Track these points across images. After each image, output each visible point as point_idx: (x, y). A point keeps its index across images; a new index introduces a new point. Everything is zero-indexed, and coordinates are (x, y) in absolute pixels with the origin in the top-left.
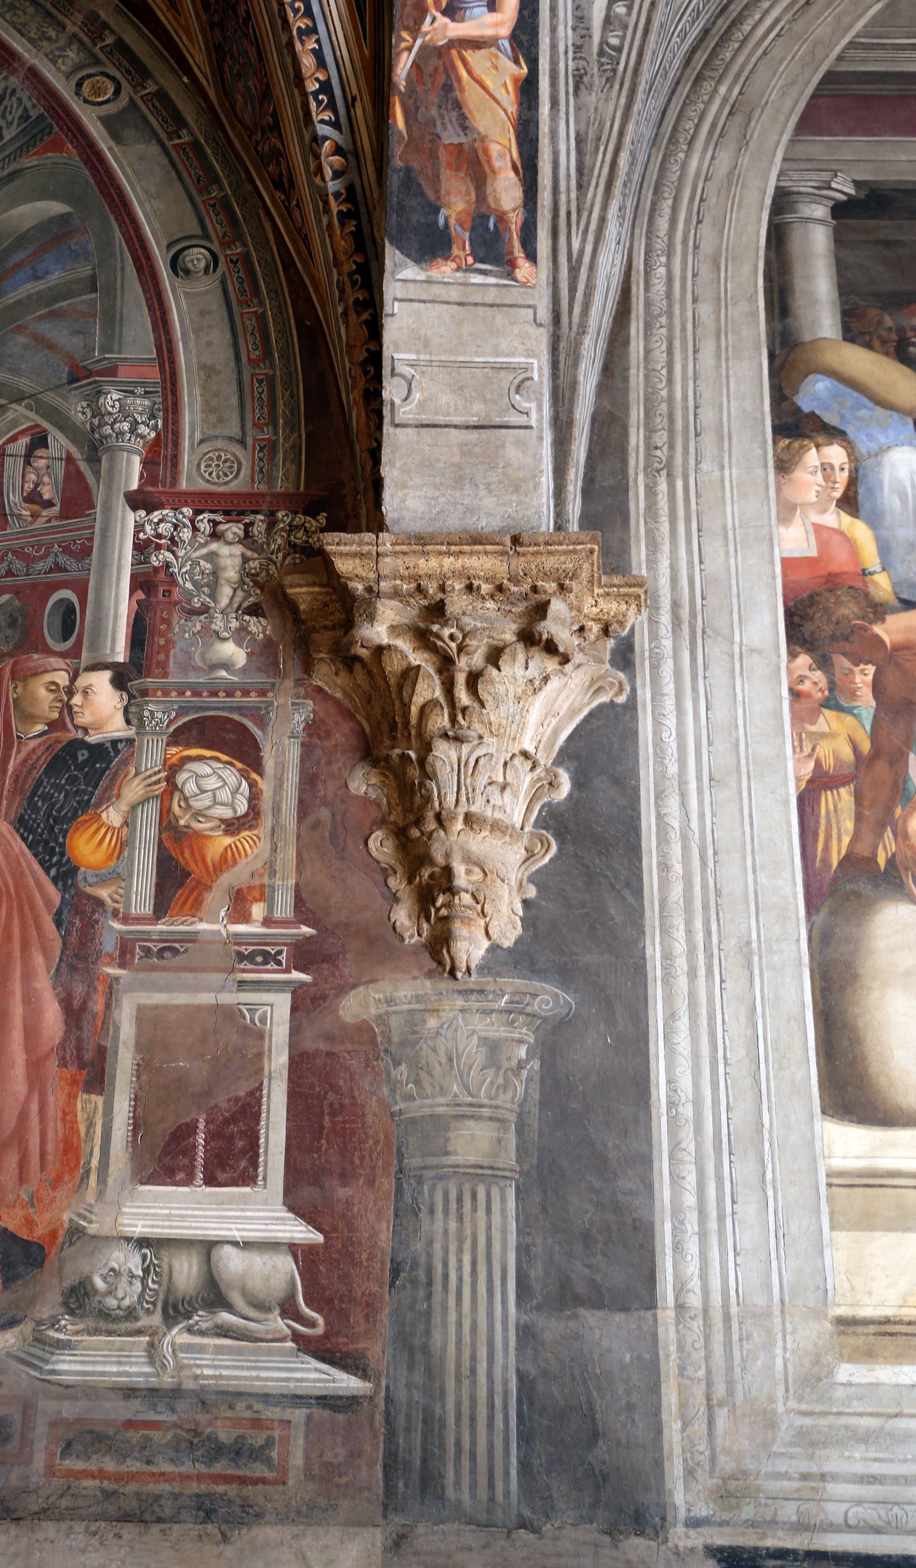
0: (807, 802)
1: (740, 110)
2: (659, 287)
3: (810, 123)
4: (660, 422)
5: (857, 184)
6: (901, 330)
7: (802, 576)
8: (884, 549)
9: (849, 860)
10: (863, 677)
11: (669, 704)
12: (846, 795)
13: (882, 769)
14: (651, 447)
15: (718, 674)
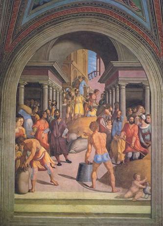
0: (16, 161)
1: (15, 72)
2: (5, 97)
3: (23, 74)
4: (4, 115)
5: (28, 82)
6: (30, 103)
7: (17, 135)
8: (26, 132)
9: (19, 167)
10: (22, 147)
11: (3, 150)
12: (19, 160)
13: (23, 157)
14: (3, 119)
15: (8, 146)
